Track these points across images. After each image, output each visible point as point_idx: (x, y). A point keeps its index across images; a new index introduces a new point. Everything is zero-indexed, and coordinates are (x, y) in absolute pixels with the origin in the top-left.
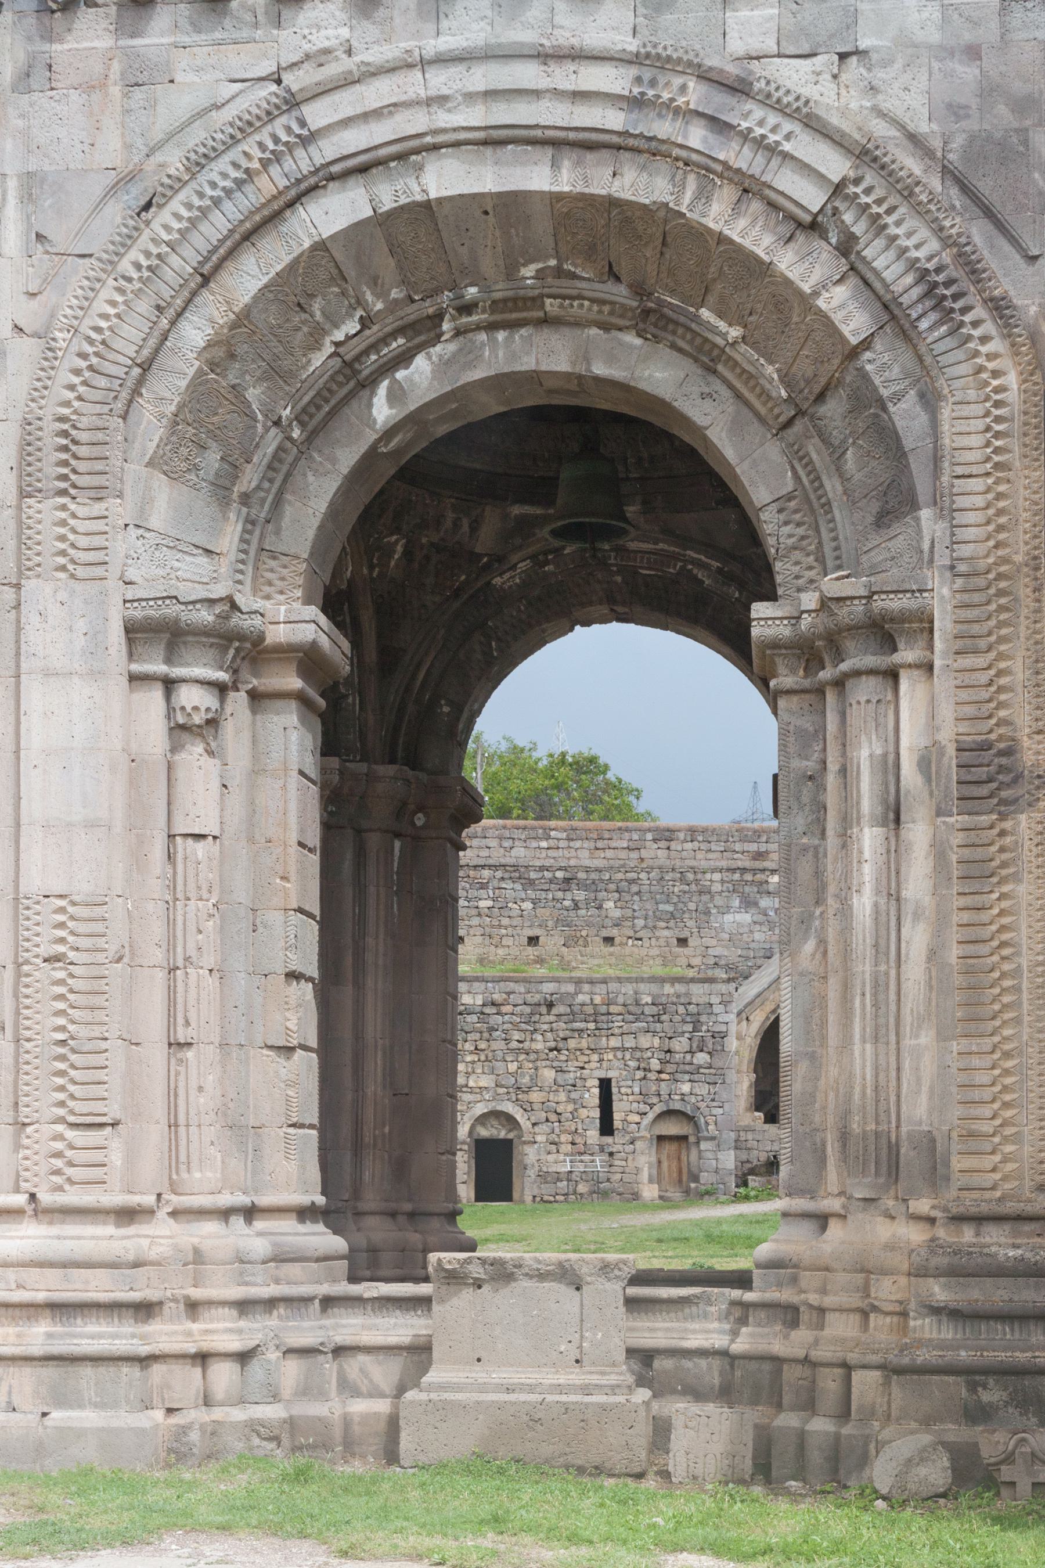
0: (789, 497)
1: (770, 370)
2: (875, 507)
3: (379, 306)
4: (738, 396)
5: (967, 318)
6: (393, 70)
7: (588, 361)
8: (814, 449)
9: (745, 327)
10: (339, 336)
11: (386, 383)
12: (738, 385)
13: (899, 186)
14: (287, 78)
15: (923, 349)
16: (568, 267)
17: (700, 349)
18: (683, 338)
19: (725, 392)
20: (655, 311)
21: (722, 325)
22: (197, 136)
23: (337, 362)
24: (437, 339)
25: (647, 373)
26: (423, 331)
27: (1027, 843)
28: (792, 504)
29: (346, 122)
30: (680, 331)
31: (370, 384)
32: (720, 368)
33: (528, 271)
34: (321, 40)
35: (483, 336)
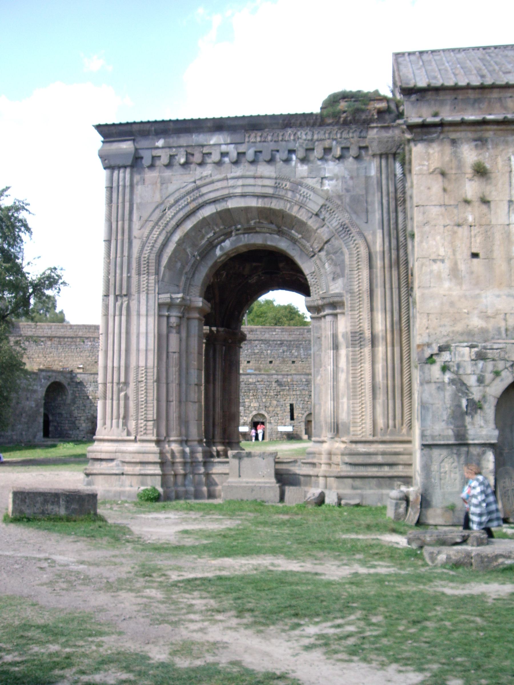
0: (314, 273)
3: (218, 230)
4: (301, 250)
5: (351, 235)
7: (266, 241)
10: (209, 236)
16: (261, 221)
22: (177, 195)
23: (208, 242)
24: (231, 236)
26: (228, 235)
29: (210, 192)
31: (216, 246)
33: (252, 223)
34: (205, 174)
35: (242, 236)
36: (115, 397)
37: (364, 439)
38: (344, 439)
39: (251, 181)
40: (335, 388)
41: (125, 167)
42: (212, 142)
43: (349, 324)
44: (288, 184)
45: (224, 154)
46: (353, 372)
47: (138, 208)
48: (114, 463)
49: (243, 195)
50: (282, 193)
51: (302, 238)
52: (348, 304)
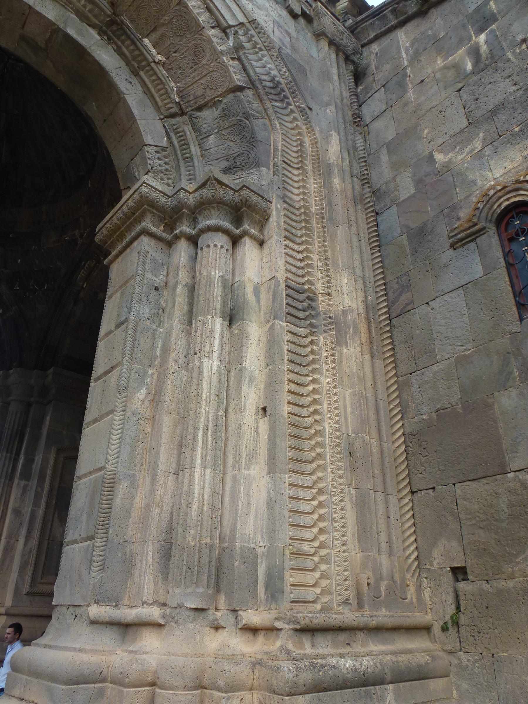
0: (164, 149)
1: (173, 85)
2: (224, 164)
9: (168, 58)
13: (265, 44)
17: (135, 58)
18: (127, 48)
19: (138, 86)
20: (118, 24)
25: (98, 52)
27: (324, 353)
28: (165, 153)
30: (128, 42)
32: (142, 73)
37: (334, 619)
40: (222, 429)
43: (281, 265)
46: (293, 387)
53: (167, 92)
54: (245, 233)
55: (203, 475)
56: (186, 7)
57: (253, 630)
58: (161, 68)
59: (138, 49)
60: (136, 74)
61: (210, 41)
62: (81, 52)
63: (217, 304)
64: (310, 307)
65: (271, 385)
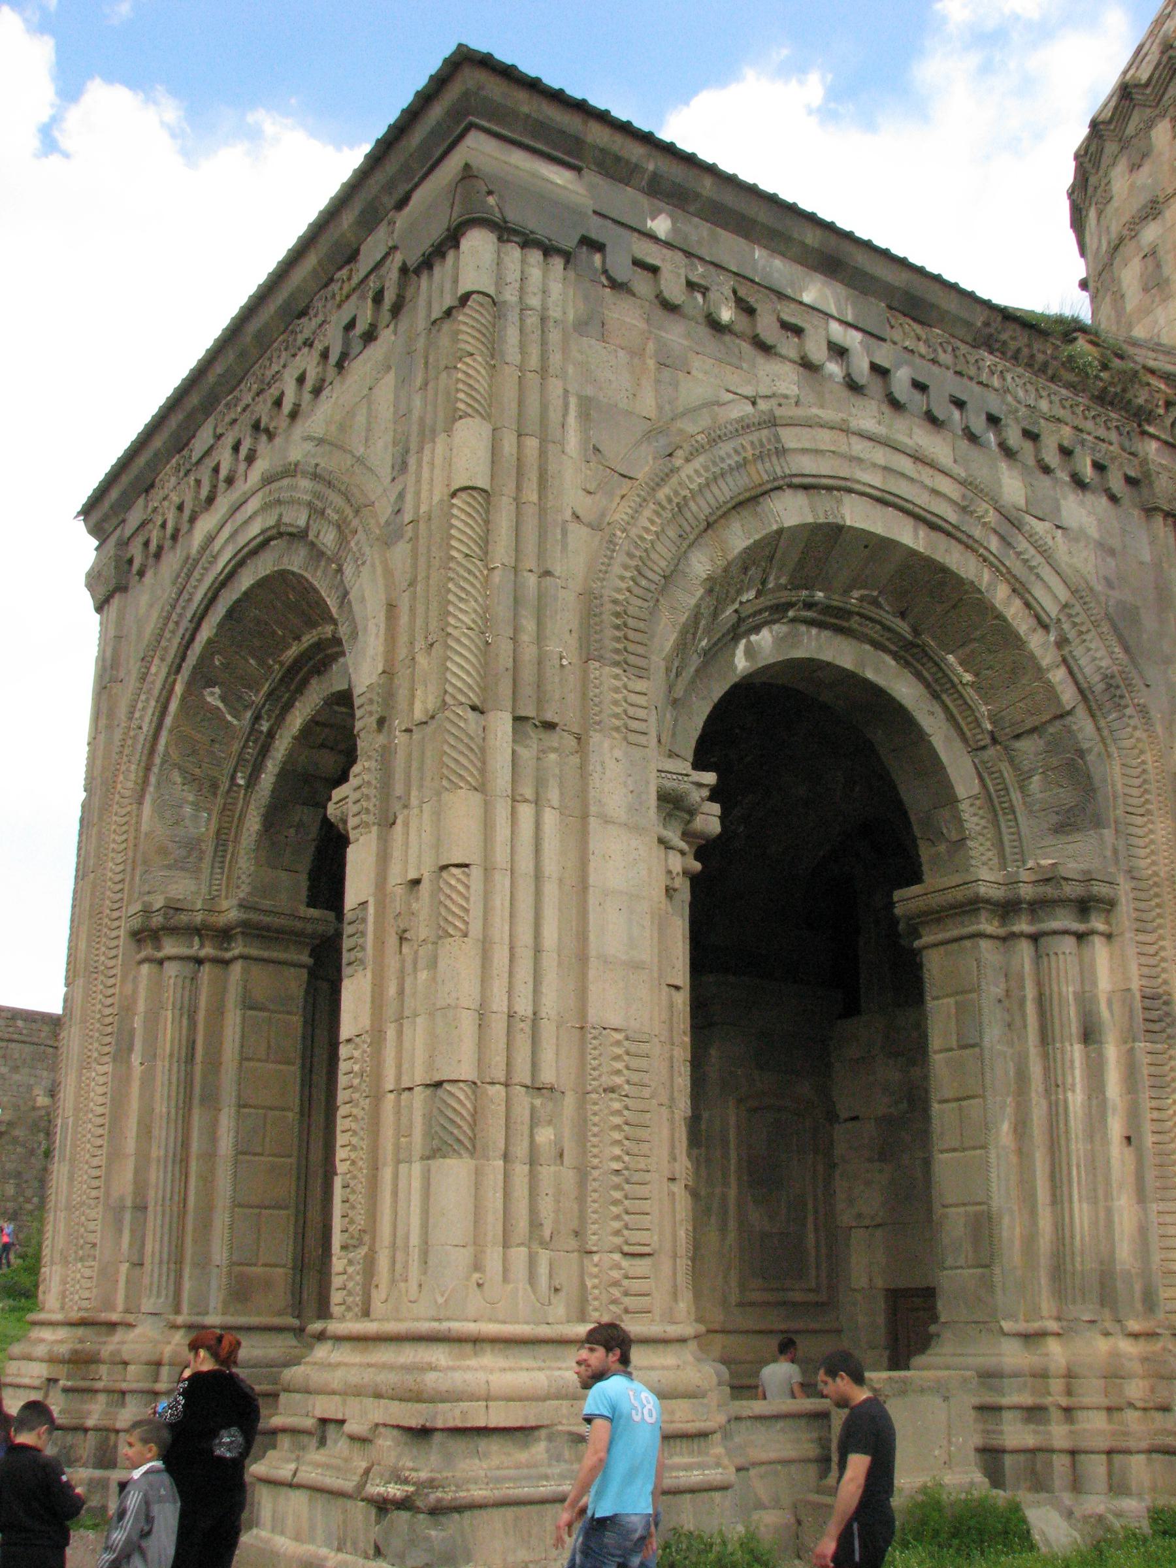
1: (983, 709)
2: (1054, 819)
4: (951, 718)
6: (832, 428)
8: (1005, 767)
9: (977, 675)
10: (744, 598)
11: (744, 641)
12: (955, 711)
14: (763, 405)
15: (1102, 723)
19: (941, 715)
21: (960, 669)
30: (930, 664)
32: (944, 697)
36: (521, 1150)
38: (1134, 1326)
39: (905, 465)
41: (548, 251)
42: (807, 298)
43: (1134, 970)
44: (991, 511)
45: (839, 352)
46: (1156, 1115)
47: (585, 416)
48: (539, 1449)
49: (882, 500)
50: (977, 533)
51: (972, 685)
52: (1125, 909)
53: (976, 720)
54: (1092, 932)
55: (1081, 1210)
56: (1005, 620)
57: (1135, 1336)
58: (969, 689)
59: (941, 669)
60: (936, 696)
61: (1032, 657)
62: (878, 693)
63: (1074, 1028)
64: (1167, 1014)
65: (1133, 1114)
